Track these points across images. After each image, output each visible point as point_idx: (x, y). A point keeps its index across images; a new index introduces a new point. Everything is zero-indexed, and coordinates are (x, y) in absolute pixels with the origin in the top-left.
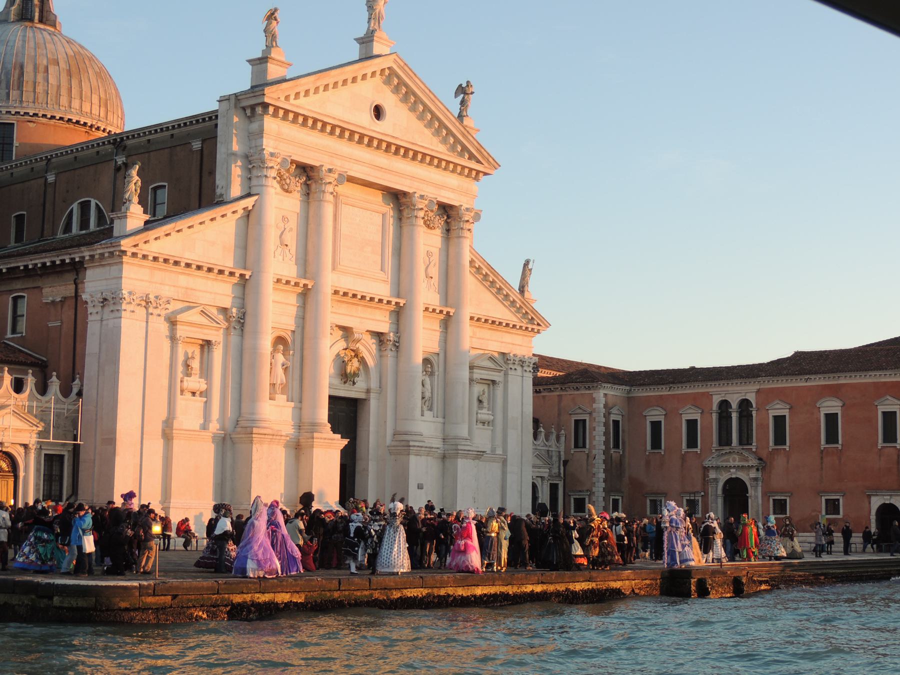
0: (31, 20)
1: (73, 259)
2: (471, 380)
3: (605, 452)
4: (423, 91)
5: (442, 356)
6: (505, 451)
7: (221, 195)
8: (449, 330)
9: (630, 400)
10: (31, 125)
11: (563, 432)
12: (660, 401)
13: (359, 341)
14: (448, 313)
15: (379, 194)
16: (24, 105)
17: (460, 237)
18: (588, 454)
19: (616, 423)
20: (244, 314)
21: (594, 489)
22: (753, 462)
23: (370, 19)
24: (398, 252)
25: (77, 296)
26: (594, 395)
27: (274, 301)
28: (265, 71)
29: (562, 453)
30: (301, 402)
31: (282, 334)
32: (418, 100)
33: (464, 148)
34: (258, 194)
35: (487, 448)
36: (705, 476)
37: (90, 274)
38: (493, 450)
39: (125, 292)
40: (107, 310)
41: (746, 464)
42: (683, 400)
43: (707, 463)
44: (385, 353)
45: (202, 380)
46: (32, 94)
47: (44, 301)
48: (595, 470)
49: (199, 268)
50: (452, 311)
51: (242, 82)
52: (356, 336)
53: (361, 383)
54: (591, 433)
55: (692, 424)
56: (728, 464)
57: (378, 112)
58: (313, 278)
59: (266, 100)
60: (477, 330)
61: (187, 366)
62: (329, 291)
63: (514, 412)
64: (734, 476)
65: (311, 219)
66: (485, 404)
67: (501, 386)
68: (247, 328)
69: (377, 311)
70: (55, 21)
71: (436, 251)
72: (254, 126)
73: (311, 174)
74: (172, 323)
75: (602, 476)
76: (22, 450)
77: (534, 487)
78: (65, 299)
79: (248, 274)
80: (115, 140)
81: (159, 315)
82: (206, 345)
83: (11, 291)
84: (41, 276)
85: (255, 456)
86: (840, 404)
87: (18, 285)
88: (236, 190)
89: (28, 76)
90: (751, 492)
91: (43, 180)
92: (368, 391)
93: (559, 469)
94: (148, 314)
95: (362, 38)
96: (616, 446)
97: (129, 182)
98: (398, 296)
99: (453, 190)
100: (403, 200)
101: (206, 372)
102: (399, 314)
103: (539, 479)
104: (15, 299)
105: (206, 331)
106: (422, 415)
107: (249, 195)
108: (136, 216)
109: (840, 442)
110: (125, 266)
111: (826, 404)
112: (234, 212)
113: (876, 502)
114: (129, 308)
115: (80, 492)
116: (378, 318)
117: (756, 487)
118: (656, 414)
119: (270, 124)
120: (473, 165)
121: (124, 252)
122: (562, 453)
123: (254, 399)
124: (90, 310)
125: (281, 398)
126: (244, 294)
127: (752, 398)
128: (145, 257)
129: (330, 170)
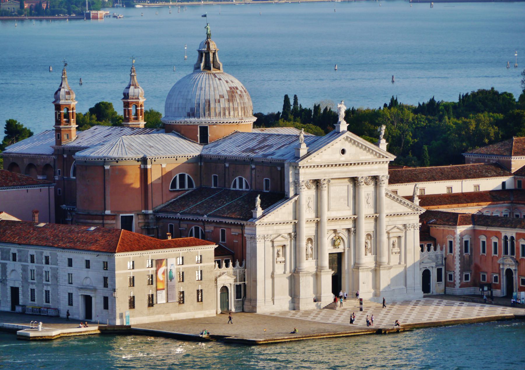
0: (210, 69)
1: (241, 224)
2: (389, 238)
5: (375, 232)
8: (378, 222)
9: (474, 231)
10: (215, 126)
11: (444, 245)
12: (484, 233)
15: (347, 180)
17: (380, 187)
19: (466, 242)
20: (296, 234)
21: (455, 271)
25: (242, 234)
26: (455, 231)
27: (306, 227)
30: (317, 259)
31: (310, 237)
33: (380, 154)
36: (499, 267)
37: (246, 227)
38: (400, 263)
39: (257, 236)
43: (499, 262)
47: (232, 234)
52: (338, 232)
55: (495, 244)
57: (343, 152)
59: (299, 166)
61: (278, 254)
62: (326, 218)
63: (410, 246)
64: (508, 268)
66: (396, 245)
68: (297, 239)
74: (272, 242)
78: (239, 234)
80: (251, 159)
82: (284, 246)
83: (220, 228)
85: (301, 281)
87: (223, 226)
88: (292, 194)
89: (212, 106)
90: (514, 276)
91: (223, 165)
92: (344, 250)
93: (442, 262)
94: (265, 241)
96: (466, 251)
99: (376, 170)
101: (284, 255)
103: (431, 268)
107: (296, 195)
114: (259, 240)
115: (247, 296)
116: (347, 223)
117: (515, 273)
118: (483, 238)
119: (301, 171)
120: (385, 160)
123: (300, 262)
124: (247, 239)
125: (310, 259)
126: (296, 228)
127: (514, 236)
128: (263, 224)
129: (324, 180)
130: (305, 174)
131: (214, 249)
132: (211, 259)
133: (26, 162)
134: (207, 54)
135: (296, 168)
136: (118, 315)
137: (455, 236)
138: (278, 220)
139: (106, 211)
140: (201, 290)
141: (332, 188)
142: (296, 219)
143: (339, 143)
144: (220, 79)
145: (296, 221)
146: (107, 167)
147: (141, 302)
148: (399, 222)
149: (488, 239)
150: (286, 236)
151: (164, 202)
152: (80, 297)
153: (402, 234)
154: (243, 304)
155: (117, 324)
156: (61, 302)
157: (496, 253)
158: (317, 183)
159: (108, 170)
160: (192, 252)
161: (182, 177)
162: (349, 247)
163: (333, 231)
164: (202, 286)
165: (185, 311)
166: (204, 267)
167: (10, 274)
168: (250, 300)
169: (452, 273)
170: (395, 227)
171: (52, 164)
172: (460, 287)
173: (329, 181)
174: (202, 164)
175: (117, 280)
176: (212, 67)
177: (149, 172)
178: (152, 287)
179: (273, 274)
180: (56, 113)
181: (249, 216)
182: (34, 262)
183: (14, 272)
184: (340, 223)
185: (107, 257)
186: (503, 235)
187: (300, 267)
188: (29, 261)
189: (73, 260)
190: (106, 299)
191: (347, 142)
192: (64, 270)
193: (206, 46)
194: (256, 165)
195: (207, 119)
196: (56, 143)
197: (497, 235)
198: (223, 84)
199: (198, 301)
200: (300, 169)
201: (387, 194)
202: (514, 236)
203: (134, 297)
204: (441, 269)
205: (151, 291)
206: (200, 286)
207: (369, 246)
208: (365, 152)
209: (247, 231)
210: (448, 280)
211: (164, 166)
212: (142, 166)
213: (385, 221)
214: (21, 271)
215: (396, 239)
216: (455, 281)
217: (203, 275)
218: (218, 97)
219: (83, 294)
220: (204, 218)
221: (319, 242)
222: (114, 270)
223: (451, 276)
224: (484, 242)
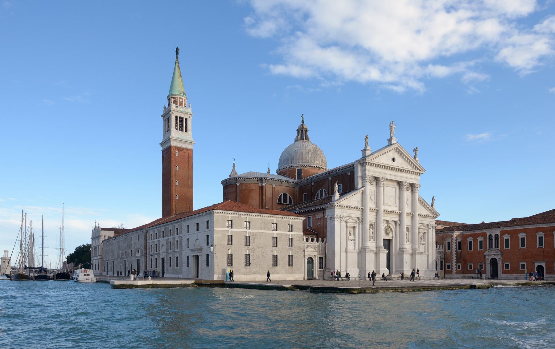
2: (419, 232)
3: (456, 251)
5: (411, 226)
6: (428, 252)
7: (356, 188)
8: (413, 219)
12: (471, 236)
13: (390, 223)
14: (413, 214)
18: (451, 252)
21: (453, 262)
22: (499, 253)
23: (391, 134)
31: (371, 223)
32: (404, 155)
33: (416, 167)
34: (365, 187)
35: (423, 251)
36: (485, 257)
38: (425, 252)
40: (331, 220)
43: (485, 254)
44: (397, 226)
45: (354, 237)
48: (453, 257)
49: (352, 207)
50: (413, 213)
51: (359, 156)
52: (389, 222)
54: (452, 246)
55: (481, 242)
56: (492, 254)
57: (394, 160)
58: (379, 208)
59: (366, 161)
63: (430, 241)
64: (493, 257)
65: (378, 192)
66: (423, 239)
67: (427, 233)
68: (363, 222)
69: (395, 215)
72: (363, 168)
73: (377, 179)
74: (346, 222)
76: (314, 257)
77: (436, 262)
79: (363, 208)
81: (343, 221)
84: (315, 212)
86: (525, 234)
88: (360, 186)
90: (498, 262)
95: (389, 139)
97: (335, 187)
98: (400, 211)
99: (413, 179)
100: (400, 183)
101: (354, 235)
102: (400, 215)
104: (309, 218)
105: (354, 224)
106: (407, 243)
107: (363, 187)
108: (337, 195)
109: (525, 246)
110: (335, 209)
112: (360, 192)
114: (337, 219)
118: (471, 239)
119: (367, 167)
120: (419, 171)
121: (335, 205)
125: (372, 240)
126: (362, 214)
127: (499, 234)
128: (340, 206)
129: (382, 178)
130: (369, 171)
132: (300, 229)
138: (349, 205)
140: (292, 256)
141: (386, 188)
142: (362, 207)
149: (475, 240)
150: (356, 219)
153: (426, 231)
157: (481, 248)
158: (377, 179)
160: (285, 221)
162: (396, 235)
163: (386, 222)
164: (292, 252)
165: (278, 273)
166: (294, 235)
169: (450, 264)
172: (456, 273)
178: (249, 248)
179: (346, 248)
181: (329, 199)
184: (390, 215)
186: (488, 235)
187: (365, 245)
197: (484, 235)
199: (289, 265)
202: (499, 234)
204: (442, 261)
205: (248, 251)
206: (291, 252)
207: (408, 237)
208: (406, 163)
210: (447, 269)
213: (417, 219)
215: (423, 234)
216: (452, 269)
217: (293, 243)
221: (377, 228)
222: (213, 227)
224: (470, 243)
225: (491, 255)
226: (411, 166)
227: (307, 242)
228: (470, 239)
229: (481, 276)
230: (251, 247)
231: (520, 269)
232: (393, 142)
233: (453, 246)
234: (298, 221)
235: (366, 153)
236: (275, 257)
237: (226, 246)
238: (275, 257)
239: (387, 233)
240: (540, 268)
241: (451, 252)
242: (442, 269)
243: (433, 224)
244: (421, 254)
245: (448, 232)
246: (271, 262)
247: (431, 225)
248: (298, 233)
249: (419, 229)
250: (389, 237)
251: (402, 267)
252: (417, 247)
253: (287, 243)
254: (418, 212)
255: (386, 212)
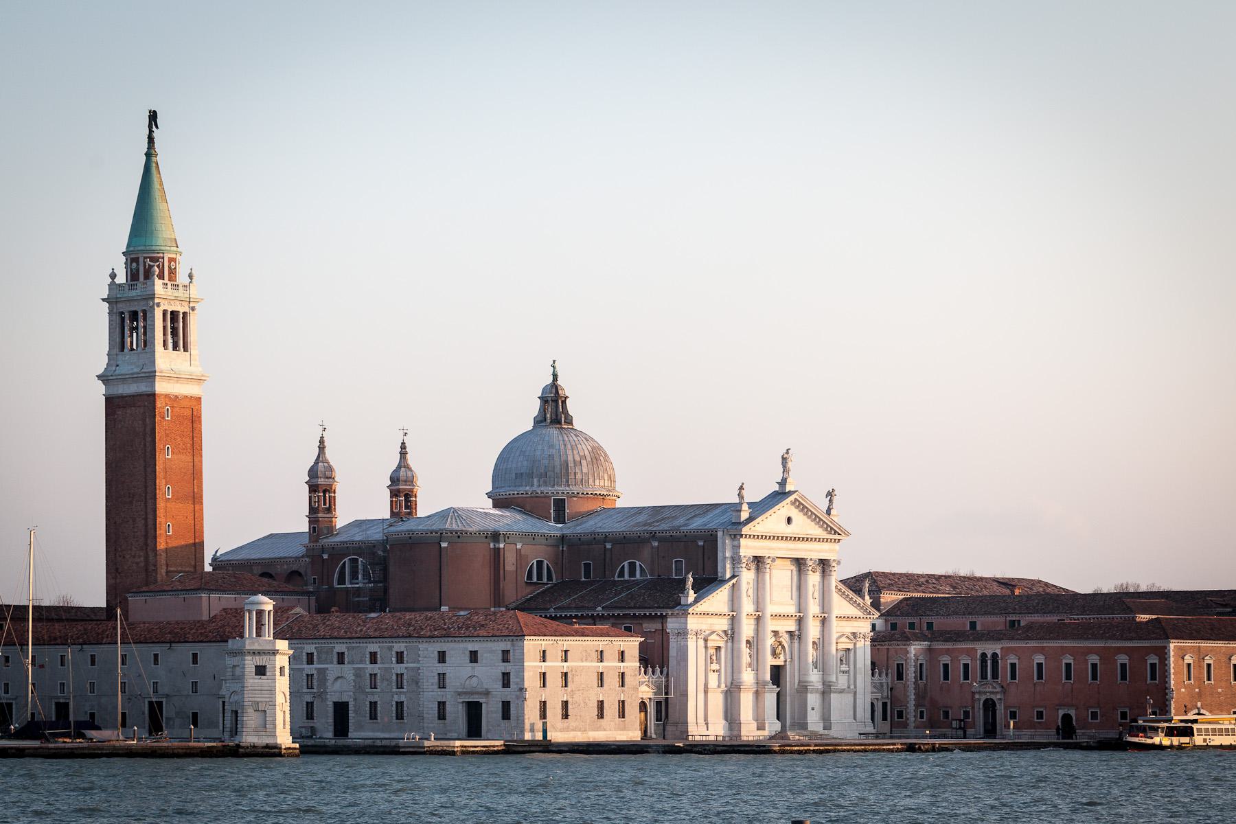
0: (560, 423)
1: (662, 614)
2: (837, 650)
4: (811, 506)
6: (855, 687)
8: (825, 625)
10: (575, 499)
11: (890, 671)
12: (948, 651)
16: (571, 487)
19: (921, 665)
21: (908, 705)
22: (999, 689)
24: (799, 588)
28: (740, 516)
29: (889, 684)
31: (748, 639)
33: (832, 528)
36: (973, 697)
37: (669, 620)
38: (849, 687)
41: (995, 690)
42: (962, 651)
46: (574, 480)
50: (826, 615)
52: (780, 635)
53: (782, 656)
54: (906, 672)
55: (966, 666)
57: (789, 520)
60: (840, 622)
63: (860, 664)
66: (844, 662)
67: (853, 651)
68: (735, 639)
70: (572, 420)
71: (817, 584)
72: (736, 543)
74: (706, 641)
75: (913, 697)
77: (872, 704)
83: (624, 624)
88: (728, 575)
91: (603, 546)
94: (697, 638)
96: (921, 679)
98: (799, 612)
99: (826, 551)
101: (718, 661)
102: (800, 621)
107: (733, 576)
108: (692, 595)
111: (1037, 657)
113: (1061, 713)
114: (691, 637)
115: (669, 717)
118: (946, 659)
119: (743, 541)
120: (837, 537)
122: (889, 684)
123: (740, 672)
127: (998, 652)
128: (697, 614)
129: (769, 557)
130: (747, 547)
131: (638, 643)
133: (257, 570)
134: (556, 401)
135: (737, 536)
136: (527, 726)
137: (908, 655)
138: (711, 610)
139: (442, 607)
143: (785, 508)
144: (576, 436)
145: (735, 614)
146: (444, 545)
147: (554, 711)
148: (849, 627)
150: (721, 633)
151: (519, 598)
152: (460, 706)
153: (851, 646)
154: (664, 730)
155: (526, 739)
156: (425, 716)
158: (758, 561)
159: (446, 548)
161: (540, 563)
165: (605, 730)
166: (627, 667)
167: (333, 683)
168: (675, 724)
170: (843, 635)
171: (302, 571)
173: (773, 560)
174: (564, 549)
175: (526, 675)
176: (563, 421)
177: (502, 553)
178: (566, 690)
179: (706, 686)
180: (310, 497)
182: (376, 663)
183: (340, 680)
184: (783, 622)
185: (509, 643)
188: (368, 662)
189: (447, 653)
190: (506, 706)
191: (793, 507)
192: (430, 668)
193: (554, 390)
194: (659, 542)
195: (563, 488)
196: (310, 539)
197: (970, 653)
198: (582, 443)
200: (741, 539)
201: (836, 586)
203: (545, 702)
204: (886, 703)
206: (622, 695)
209: (672, 625)
211: (519, 546)
212: (492, 545)
213: (836, 627)
214: (353, 678)
216: (907, 719)
218: (579, 459)
219: (467, 700)
220: (597, 611)
222: (522, 661)
223: (900, 715)
225: (985, 693)
226: (822, 527)
227: (645, 675)
228: (944, 659)
229: (965, 732)
230: (569, 688)
231: (1036, 720)
232: (789, 488)
233: (908, 672)
234: (631, 645)
235: (740, 516)
236: (601, 705)
237: (538, 689)
238: (601, 705)
239: (774, 654)
240: (1067, 718)
241: (906, 687)
242: (886, 720)
243: (866, 631)
244: (842, 691)
245: (899, 642)
246: (595, 712)
247: (860, 633)
248: (633, 663)
249: (837, 643)
250: (779, 662)
251: (806, 717)
252: (834, 679)
253: (616, 681)
254: (836, 612)
255: (776, 616)
